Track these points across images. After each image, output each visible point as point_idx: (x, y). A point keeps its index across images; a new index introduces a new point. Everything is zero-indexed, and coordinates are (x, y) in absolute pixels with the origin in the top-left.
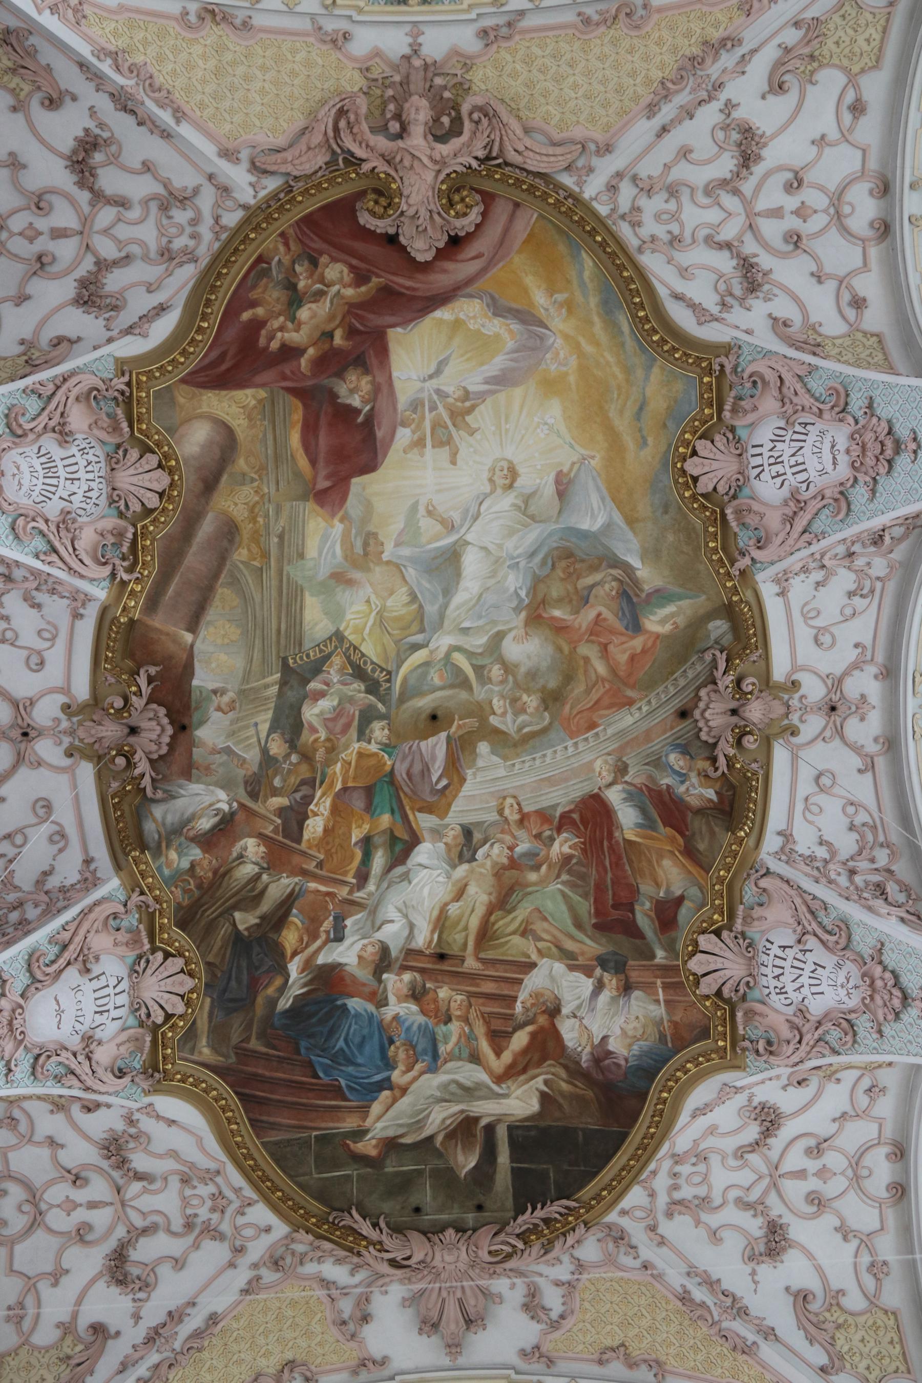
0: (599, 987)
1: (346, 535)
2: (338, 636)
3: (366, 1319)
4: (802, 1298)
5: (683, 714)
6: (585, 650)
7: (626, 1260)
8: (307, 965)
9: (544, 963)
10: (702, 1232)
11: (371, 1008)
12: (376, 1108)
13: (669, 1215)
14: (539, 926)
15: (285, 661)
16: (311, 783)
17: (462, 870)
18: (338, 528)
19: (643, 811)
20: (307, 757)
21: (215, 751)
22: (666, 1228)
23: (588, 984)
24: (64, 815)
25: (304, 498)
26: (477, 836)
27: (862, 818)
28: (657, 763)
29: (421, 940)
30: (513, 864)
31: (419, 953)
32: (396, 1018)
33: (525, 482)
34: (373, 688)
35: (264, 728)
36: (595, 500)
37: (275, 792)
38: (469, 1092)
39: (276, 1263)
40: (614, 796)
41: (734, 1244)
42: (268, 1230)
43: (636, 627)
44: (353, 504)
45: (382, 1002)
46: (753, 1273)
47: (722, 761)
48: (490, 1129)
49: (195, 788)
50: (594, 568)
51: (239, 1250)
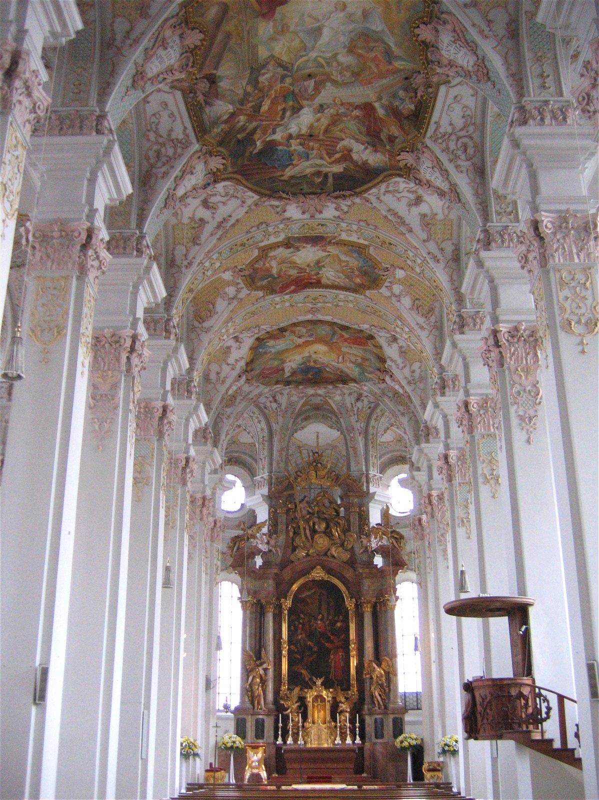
0: (366, 148)
1: (274, 26)
2: (272, 56)
3: (285, 211)
4: (423, 216)
5: (406, 79)
6: (369, 63)
7: (370, 205)
8: (263, 142)
9: (348, 140)
10: (395, 198)
11: (285, 148)
12: (287, 170)
13: (384, 194)
14: (346, 131)
15: (252, 68)
16: (263, 97)
17: (319, 115)
18: (271, 24)
19: (386, 111)
20: (261, 90)
21: (226, 90)
22: (382, 198)
23: (363, 147)
24: (172, 107)
25: (257, 17)
26: (325, 107)
27: (468, 112)
28: (394, 96)
29: (304, 131)
30: (338, 114)
31: (303, 135)
32: (295, 150)
33: (349, 9)
34: (285, 68)
35: (244, 84)
36: (378, 22)
37: (249, 102)
38: (320, 166)
39: (256, 205)
40: (377, 105)
41: (404, 202)
42: (253, 197)
43: (390, 63)
44: (277, 16)
45: (291, 146)
46: (409, 210)
47: (419, 95)
48: (326, 176)
49: (220, 102)
50: (376, 41)
51: (244, 202)
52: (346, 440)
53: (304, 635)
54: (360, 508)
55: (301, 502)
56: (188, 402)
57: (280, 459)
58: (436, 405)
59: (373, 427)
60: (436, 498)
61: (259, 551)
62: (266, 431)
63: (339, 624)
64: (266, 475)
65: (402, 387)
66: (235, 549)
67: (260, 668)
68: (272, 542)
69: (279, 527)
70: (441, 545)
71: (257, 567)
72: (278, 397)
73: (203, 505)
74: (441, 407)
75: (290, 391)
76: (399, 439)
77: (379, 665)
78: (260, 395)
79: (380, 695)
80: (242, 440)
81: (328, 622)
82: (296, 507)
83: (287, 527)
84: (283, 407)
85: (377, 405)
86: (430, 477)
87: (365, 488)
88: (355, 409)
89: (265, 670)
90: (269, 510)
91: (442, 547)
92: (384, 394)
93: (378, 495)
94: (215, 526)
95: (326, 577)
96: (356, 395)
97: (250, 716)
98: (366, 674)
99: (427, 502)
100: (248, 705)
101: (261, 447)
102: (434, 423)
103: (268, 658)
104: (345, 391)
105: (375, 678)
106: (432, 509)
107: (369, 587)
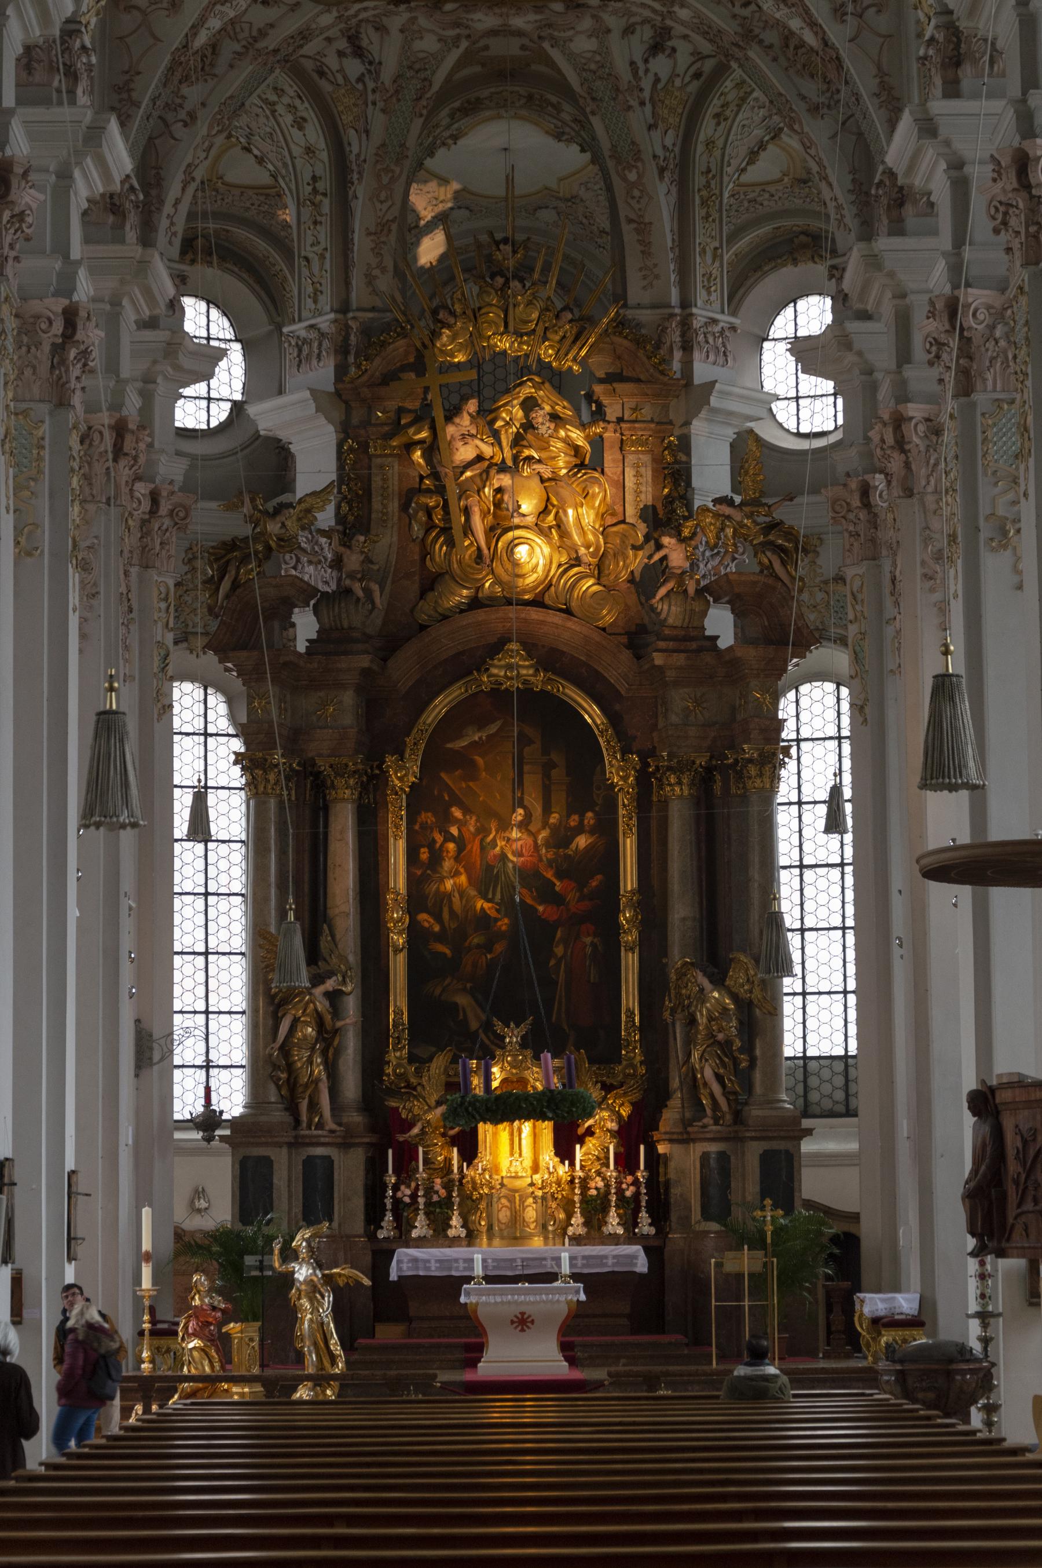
52: (609, 188)
53: (463, 879)
55: (452, 414)
56: (66, 112)
58: (928, 128)
59: (710, 144)
60: (921, 428)
61: (306, 593)
62: (324, 156)
63: (582, 841)
64: (325, 322)
65: (813, 24)
66: (225, 586)
67: (319, 991)
68: (353, 561)
69: (376, 504)
70: (932, 590)
71: (301, 647)
72: (369, 38)
73: (118, 451)
74: (943, 132)
75: (413, 19)
76: (804, 176)
77: (719, 980)
78: (304, 35)
79: (719, 1078)
80: (231, 177)
81: (544, 834)
83: (405, 507)
84: (387, 75)
85: (721, 71)
86: (904, 356)
87: (676, 366)
88: (647, 84)
89: (334, 997)
90: (340, 445)
91: (937, 596)
92: (749, 35)
93: (724, 394)
94: (154, 511)
95: (539, 681)
96: (647, 33)
97: (285, 1150)
98: (673, 1011)
99: (890, 440)
100: (278, 1116)
101: (307, 212)
102: (918, 182)
103: (343, 959)
104: (611, 21)
105: (702, 1020)
106: (907, 465)
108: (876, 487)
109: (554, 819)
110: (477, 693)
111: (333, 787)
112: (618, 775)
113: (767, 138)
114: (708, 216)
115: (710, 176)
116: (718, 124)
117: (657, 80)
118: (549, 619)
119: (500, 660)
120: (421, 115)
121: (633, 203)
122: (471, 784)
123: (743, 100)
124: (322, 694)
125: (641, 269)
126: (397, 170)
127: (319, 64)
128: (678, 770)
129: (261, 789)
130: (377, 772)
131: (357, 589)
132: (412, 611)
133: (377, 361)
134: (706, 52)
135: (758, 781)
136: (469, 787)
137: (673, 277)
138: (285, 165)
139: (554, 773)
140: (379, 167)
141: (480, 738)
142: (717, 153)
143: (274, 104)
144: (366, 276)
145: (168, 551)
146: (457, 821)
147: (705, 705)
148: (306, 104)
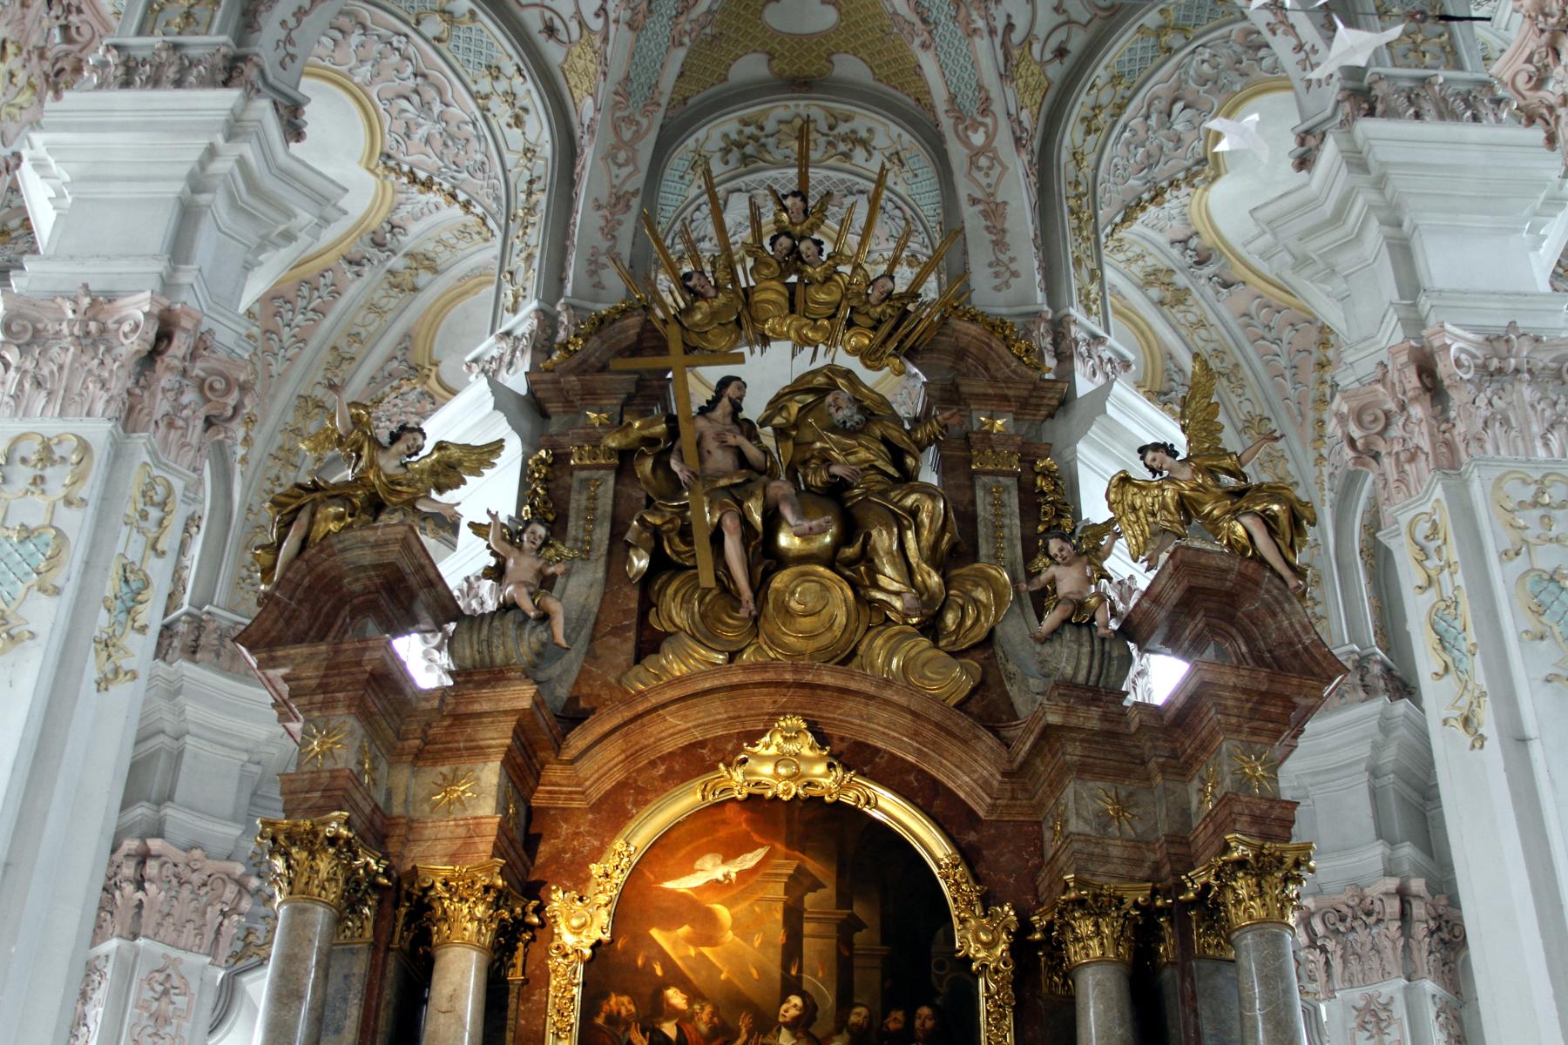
54: (1028, 459)
57: (604, 245)
62: (547, 150)
68: (522, 566)
69: (574, 528)
82: (674, 432)
107: (1103, 820)
108: (1447, 347)
109: (858, 1015)
110: (722, 804)
111: (445, 917)
112: (977, 940)
113: (1146, 196)
114: (1080, 229)
115: (1081, 189)
116: (1088, 132)
117: (1010, 27)
118: (853, 686)
119: (767, 746)
120: (681, 44)
121: (979, 176)
122: (706, 951)
123: (1121, 108)
124: (445, 769)
125: (990, 265)
126: (645, 122)
127: (548, 14)
128: (1094, 906)
129: (300, 885)
130: (536, 920)
131: (526, 604)
132: (619, 681)
133: (595, 342)
134: (1074, 16)
135: (1257, 903)
136: (702, 955)
137: (1038, 277)
138: (497, 199)
139: (859, 937)
140: (619, 114)
141: (726, 876)
142: (1088, 172)
143: (487, 97)
144: (591, 262)
145: (184, 435)
146: (674, 1013)
147: (1135, 811)
148: (530, 84)
